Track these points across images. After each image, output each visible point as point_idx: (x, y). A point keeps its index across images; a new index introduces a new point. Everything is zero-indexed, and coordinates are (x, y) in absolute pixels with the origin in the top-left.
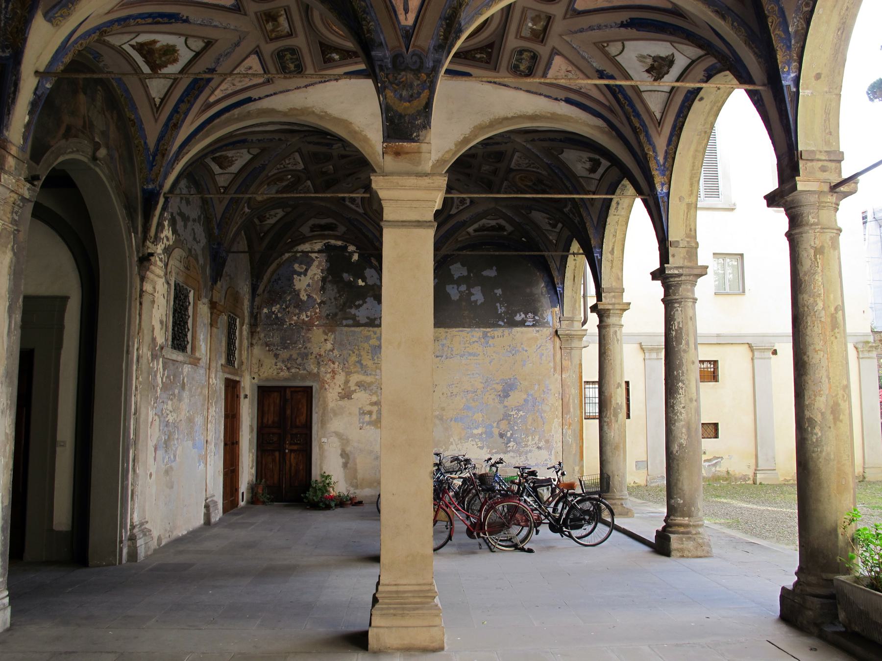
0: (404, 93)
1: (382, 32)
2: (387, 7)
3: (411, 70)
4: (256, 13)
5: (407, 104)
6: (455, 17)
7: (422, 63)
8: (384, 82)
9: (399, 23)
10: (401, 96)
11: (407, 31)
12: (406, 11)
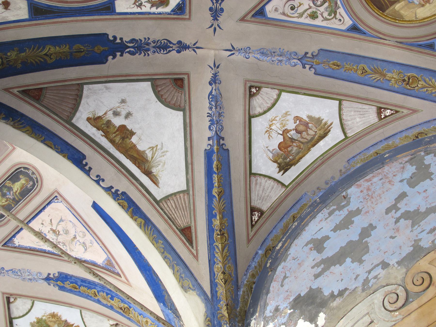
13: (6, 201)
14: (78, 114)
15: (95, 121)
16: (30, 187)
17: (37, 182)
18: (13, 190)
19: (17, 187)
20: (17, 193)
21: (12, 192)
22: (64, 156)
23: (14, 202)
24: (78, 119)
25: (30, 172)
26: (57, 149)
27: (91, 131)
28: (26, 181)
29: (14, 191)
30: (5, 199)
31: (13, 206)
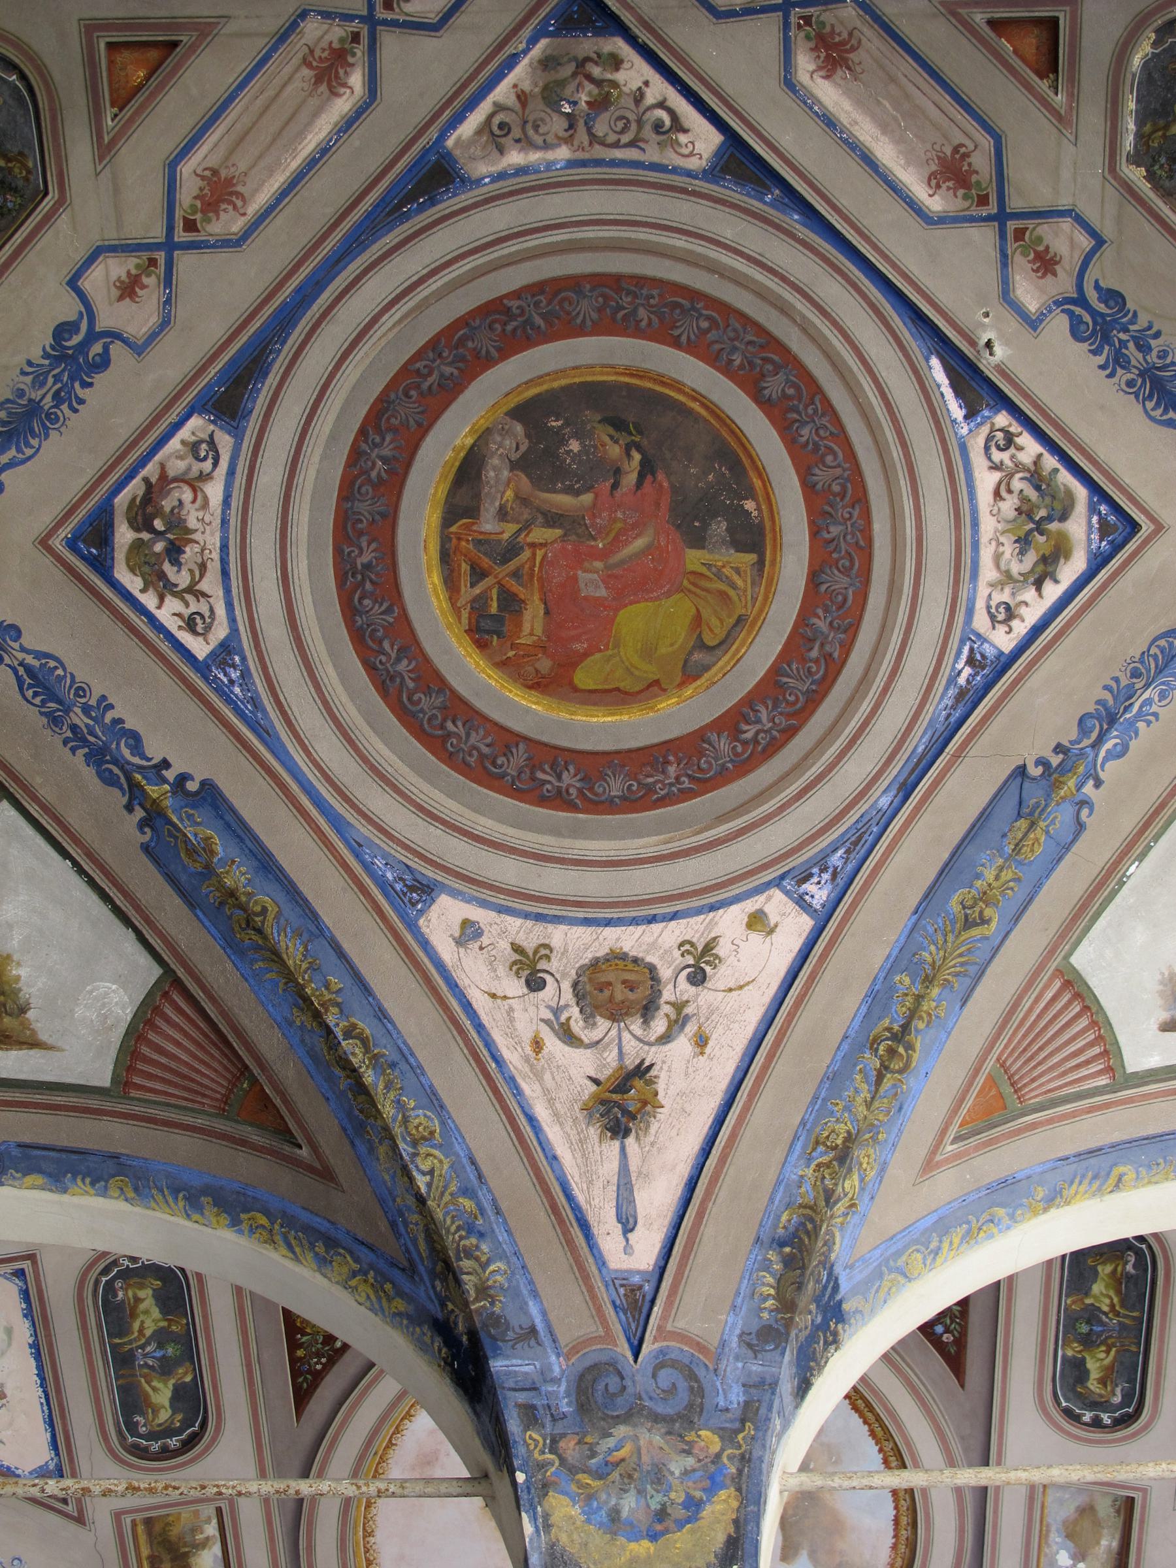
0: (629, 1504)
1: (535, 1294)
2: (554, 1208)
3: (656, 1418)
5: (644, 1547)
6: (814, 1234)
7: (698, 1391)
8: (542, 1466)
9: (601, 1263)
10: (614, 1515)
11: (633, 1290)
12: (628, 1224)
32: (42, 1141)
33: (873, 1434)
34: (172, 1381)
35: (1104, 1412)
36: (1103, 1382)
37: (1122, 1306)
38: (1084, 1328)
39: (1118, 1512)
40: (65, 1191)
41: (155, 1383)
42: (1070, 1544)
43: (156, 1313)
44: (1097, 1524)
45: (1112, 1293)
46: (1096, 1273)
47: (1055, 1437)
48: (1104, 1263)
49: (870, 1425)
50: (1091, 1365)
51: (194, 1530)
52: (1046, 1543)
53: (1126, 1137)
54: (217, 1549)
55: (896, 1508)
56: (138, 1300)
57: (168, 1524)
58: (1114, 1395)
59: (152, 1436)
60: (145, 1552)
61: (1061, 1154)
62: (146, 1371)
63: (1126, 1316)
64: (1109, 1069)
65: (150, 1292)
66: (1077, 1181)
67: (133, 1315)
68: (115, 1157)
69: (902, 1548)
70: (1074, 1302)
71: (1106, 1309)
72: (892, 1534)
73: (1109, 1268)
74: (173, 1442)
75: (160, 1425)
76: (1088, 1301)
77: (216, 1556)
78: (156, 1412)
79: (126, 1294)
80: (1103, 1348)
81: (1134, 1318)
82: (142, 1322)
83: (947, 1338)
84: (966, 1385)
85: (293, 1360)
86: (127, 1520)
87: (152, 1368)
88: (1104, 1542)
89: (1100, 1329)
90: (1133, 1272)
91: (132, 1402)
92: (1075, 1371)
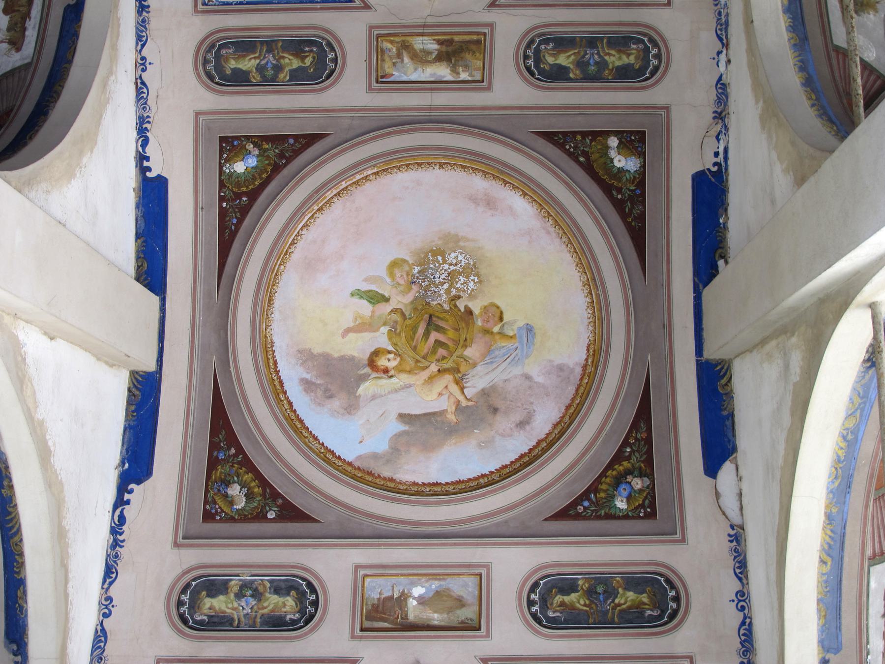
4: (491, 26)
13: (283, 57)
14: (18, 64)
15: (16, 43)
16: (230, 48)
17: (212, 46)
18: (258, 65)
19: (248, 64)
20: (257, 55)
21: (263, 62)
22: (80, 27)
23: (274, 47)
24: (23, 59)
25: (210, 67)
26: (73, 42)
27: (31, 34)
28: (227, 60)
29: (258, 61)
30: (282, 60)
31: (280, 44)
32: (804, 7)
33: (504, 467)
34: (572, 67)
35: (540, 607)
36: (562, 604)
37: (620, 611)
38: (600, 589)
39: (463, 622)
40: (784, 12)
41: (573, 57)
42: (431, 594)
43: (618, 63)
44: (450, 610)
45: (628, 604)
46: (642, 593)
47: (519, 578)
48: (649, 597)
49: (510, 465)
50: (573, 596)
51: (466, 67)
52: (430, 579)
53: (845, 566)
54: (450, 78)
55: (447, 484)
56: (628, 55)
57: (474, 53)
58: (554, 612)
59: (537, 52)
60: (457, 38)
61: (848, 524)
62: (582, 54)
63: (613, 614)
64: (874, 555)
65: (633, 62)
66: (832, 535)
67: (619, 51)
68: (806, 38)
69: (415, 489)
70: (618, 582)
71: (617, 601)
72: (426, 482)
73: (646, 600)
74: (531, 62)
75: (544, 56)
76: (620, 590)
77: (444, 77)
78: (553, 55)
79: (634, 49)
80: (587, 602)
81: (613, 618)
82: (614, 56)
83: (580, 509)
84: (547, 523)
85: (575, 133)
86: (487, 30)
87: (584, 57)
88: (436, 615)
89: (602, 599)
90: (647, 615)
91: (562, 43)
92: (569, 587)
